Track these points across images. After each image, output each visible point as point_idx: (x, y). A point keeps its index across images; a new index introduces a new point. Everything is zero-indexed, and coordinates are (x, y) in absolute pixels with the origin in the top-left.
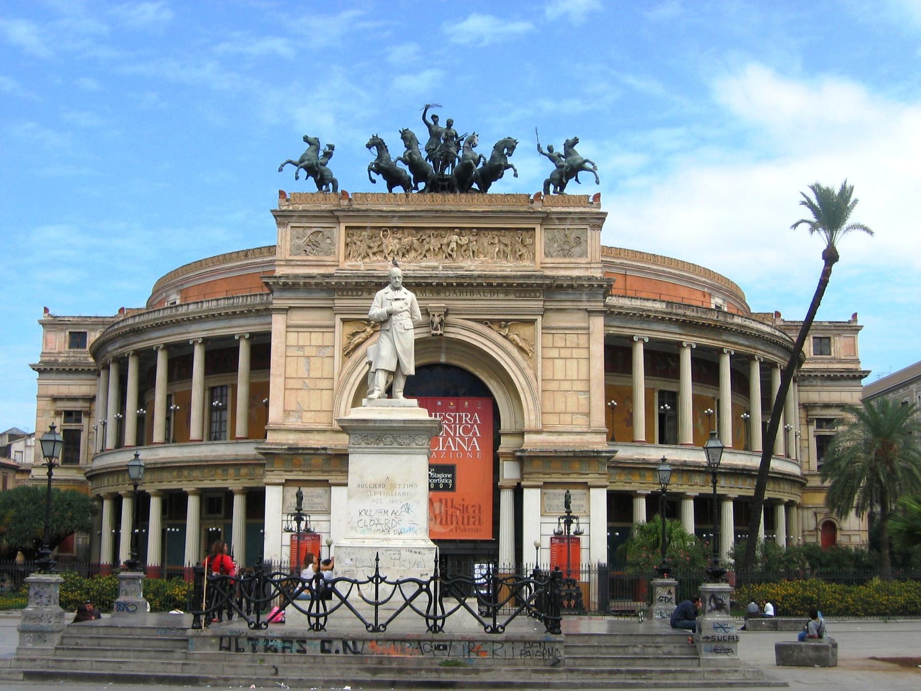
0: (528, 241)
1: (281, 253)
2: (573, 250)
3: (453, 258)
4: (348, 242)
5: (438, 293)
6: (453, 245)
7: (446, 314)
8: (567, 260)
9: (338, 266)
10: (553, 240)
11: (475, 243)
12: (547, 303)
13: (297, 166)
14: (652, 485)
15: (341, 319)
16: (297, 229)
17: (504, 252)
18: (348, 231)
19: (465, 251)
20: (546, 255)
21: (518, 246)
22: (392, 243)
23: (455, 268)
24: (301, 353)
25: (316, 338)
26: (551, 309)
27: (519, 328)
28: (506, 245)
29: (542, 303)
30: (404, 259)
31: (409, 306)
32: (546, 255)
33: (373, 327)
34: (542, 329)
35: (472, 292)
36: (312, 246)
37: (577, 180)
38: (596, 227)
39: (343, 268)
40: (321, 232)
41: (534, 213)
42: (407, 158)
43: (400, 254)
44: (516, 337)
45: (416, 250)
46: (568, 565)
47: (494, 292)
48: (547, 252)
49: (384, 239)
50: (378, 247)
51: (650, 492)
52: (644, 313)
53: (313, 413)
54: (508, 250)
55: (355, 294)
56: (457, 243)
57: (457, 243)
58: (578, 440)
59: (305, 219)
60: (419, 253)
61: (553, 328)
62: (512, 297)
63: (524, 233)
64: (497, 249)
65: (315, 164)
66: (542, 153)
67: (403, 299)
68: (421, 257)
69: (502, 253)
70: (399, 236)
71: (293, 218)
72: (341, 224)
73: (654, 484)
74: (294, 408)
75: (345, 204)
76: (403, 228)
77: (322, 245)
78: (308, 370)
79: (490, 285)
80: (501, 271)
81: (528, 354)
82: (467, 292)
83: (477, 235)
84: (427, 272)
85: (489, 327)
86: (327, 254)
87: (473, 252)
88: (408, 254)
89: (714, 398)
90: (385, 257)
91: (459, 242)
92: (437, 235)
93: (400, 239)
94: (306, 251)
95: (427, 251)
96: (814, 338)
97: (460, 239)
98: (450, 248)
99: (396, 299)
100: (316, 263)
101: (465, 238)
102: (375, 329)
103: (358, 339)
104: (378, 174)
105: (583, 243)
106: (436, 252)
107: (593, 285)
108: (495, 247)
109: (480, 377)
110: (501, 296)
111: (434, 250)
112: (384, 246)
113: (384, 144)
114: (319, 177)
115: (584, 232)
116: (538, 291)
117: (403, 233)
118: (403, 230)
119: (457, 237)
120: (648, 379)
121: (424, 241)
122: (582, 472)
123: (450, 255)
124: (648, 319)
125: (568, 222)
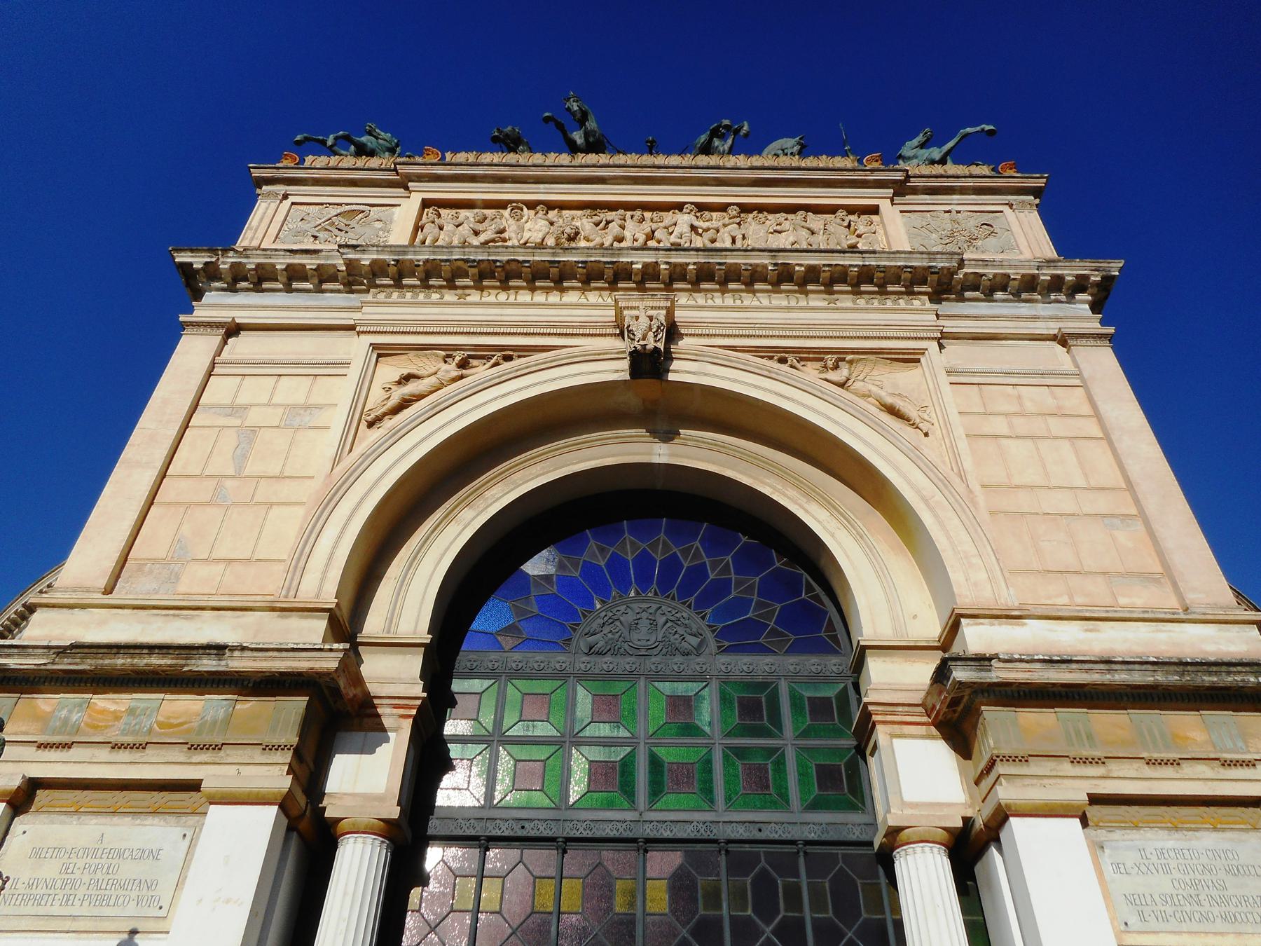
15: (375, 346)
24: (237, 422)
25: (293, 390)
27: (875, 372)
33: (463, 364)
53: (221, 567)
58: (1164, 648)
70: (552, 214)
74: (161, 553)
78: (241, 458)
85: (792, 366)
102: (464, 372)
103: (412, 388)
108: (789, 236)
109: (775, 497)
115: (997, 217)
122: (1228, 756)
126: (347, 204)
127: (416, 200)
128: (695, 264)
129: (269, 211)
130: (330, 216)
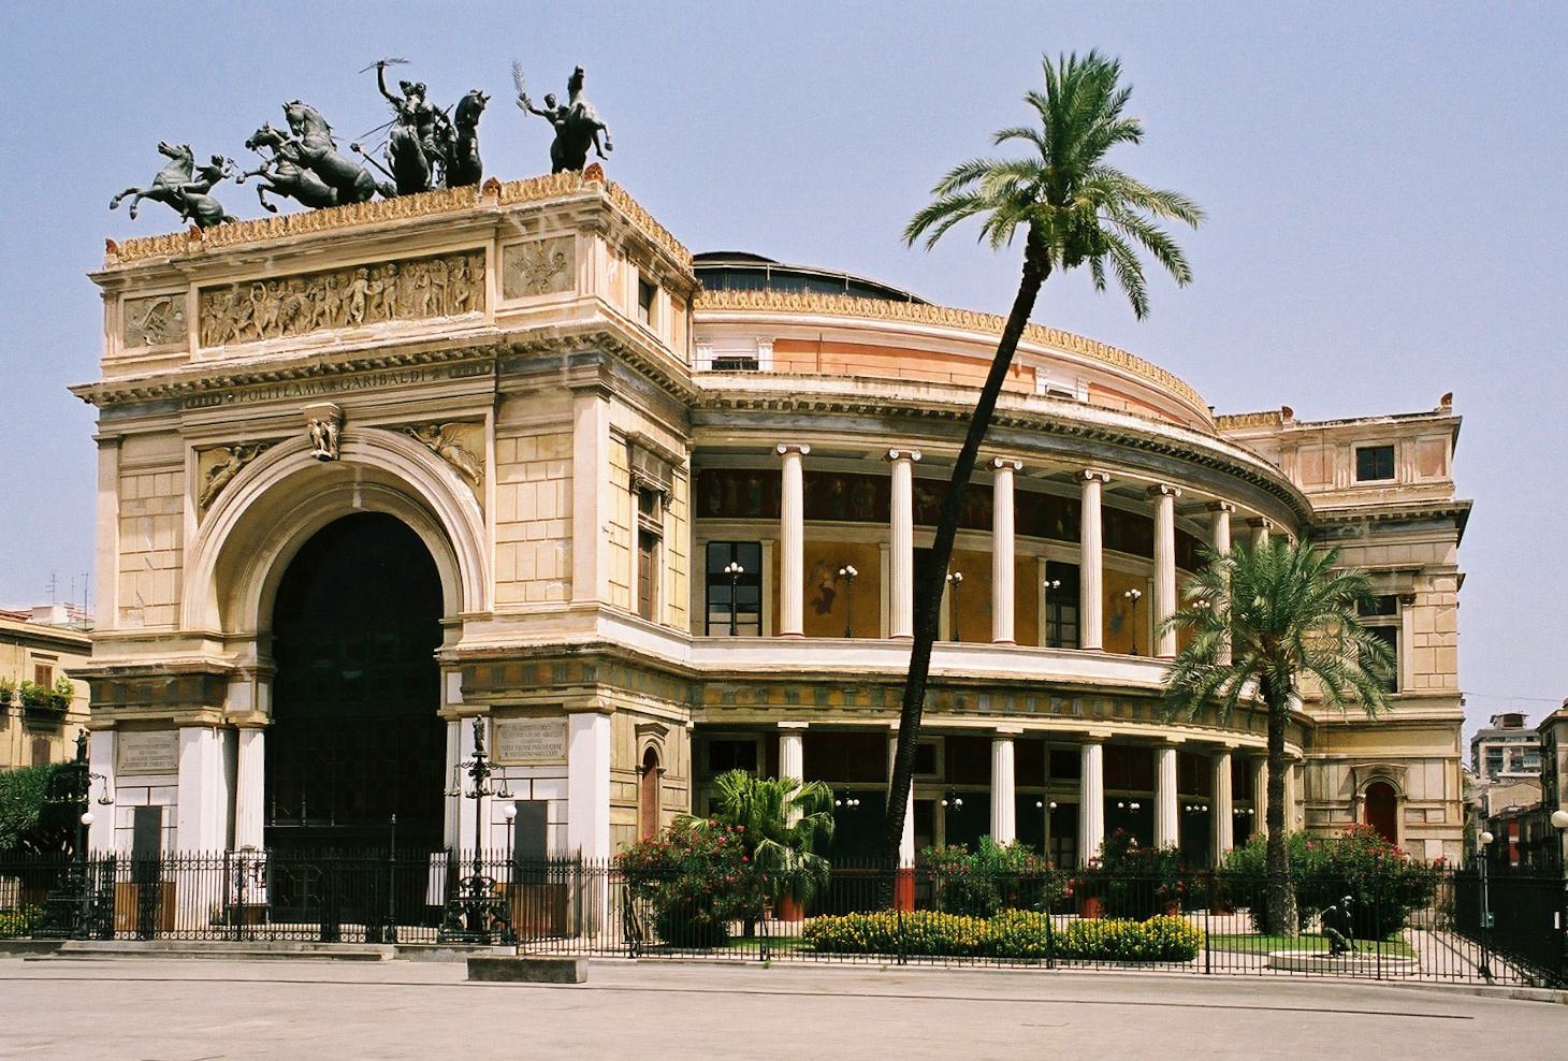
0: (478, 274)
4: (203, 315)
5: (332, 384)
6: (359, 299)
7: (341, 422)
9: (188, 358)
10: (520, 265)
11: (392, 288)
12: (502, 384)
14: (813, 712)
16: (133, 303)
17: (438, 299)
18: (207, 296)
19: (379, 306)
20: (507, 295)
21: (459, 285)
22: (269, 308)
26: (513, 393)
28: (442, 287)
32: (507, 295)
34: (496, 431)
35: (383, 378)
36: (156, 329)
38: (588, 230)
44: (454, 453)
46: (478, 865)
48: (508, 289)
49: (255, 302)
50: (249, 318)
51: (806, 725)
52: (793, 400)
54: (444, 296)
57: (364, 294)
60: (307, 320)
61: (515, 429)
62: (444, 379)
63: (472, 260)
64: (427, 297)
69: (434, 301)
70: (281, 293)
72: (192, 284)
73: (816, 710)
75: (196, 249)
76: (285, 279)
77: (171, 324)
81: (474, 479)
83: (396, 275)
85: (413, 437)
88: (293, 325)
89: (1036, 560)
90: (259, 334)
91: (367, 292)
92: (337, 284)
96: (1359, 450)
97: (370, 286)
101: (379, 283)
105: (568, 269)
106: (334, 315)
110: (428, 379)
111: (331, 311)
112: (256, 314)
117: (286, 289)
118: (286, 283)
120: (1020, 539)
123: (353, 316)
124: (821, 413)
126: (158, 296)
127: (194, 287)
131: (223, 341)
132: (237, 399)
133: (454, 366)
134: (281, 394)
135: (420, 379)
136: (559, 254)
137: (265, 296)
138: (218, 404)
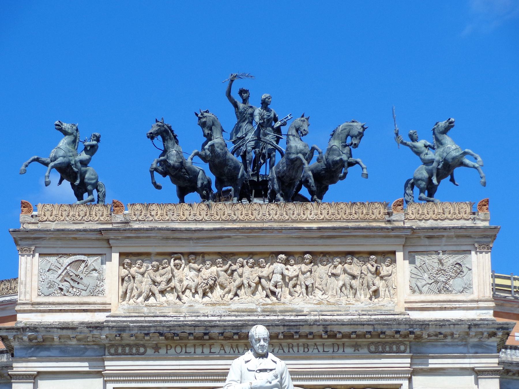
1: (25, 293)
2: (451, 282)
3: (277, 298)
8: (443, 297)
9: (109, 310)
13: (47, 164)
23: (281, 312)
28: (354, 277)
29: (409, 361)
30: (206, 299)
31: (279, 379)
36: (72, 282)
37: (452, 180)
39: (118, 313)
40: (84, 261)
41: (393, 229)
42: (208, 153)
43: (200, 291)
45: (222, 287)
47: (338, 346)
48: (414, 286)
49: (176, 271)
55: (134, 351)
56: (282, 274)
57: (282, 274)
59: (59, 243)
60: (227, 290)
64: (341, 283)
65: (73, 162)
66: (402, 143)
67: (271, 370)
68: (231, 295)
69: (348, 287)
71: (43, 242)
77: (85, 281)
79: (333, 336)
80: (347, 315)
82: (298, 346)
83: (311, 263)
84: (239, 318)
86: (92, 294)
87: (307, 287)
88: (212, 293)
93: (199, 271)
94: (61, 289)
95: (239, 288)
97: (287, 269)
98: (272, 282)
99: (261, 371)
100: (77, 307)
104: (164, 176)
107: (482, 333)
110: (349, 350)
113: (172, 131)
114: (78, 182)
116: (402, 343)
118: (203, 257)
119: (283, 266)
121: (235, 273)
123: (273, 293)
125: (444, 239)
128: (282, 333)
129: (28, 265)
130: (65, 266)
131: (141, 299)
132: (163, 351)
133: (372, 343)
134: (206, 350)
135: (341, 350)
136: (457, 264)
137: (183, 266)
138: (143, 354)
